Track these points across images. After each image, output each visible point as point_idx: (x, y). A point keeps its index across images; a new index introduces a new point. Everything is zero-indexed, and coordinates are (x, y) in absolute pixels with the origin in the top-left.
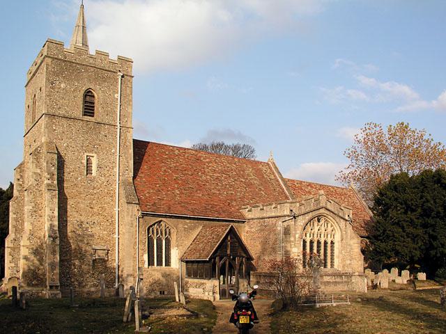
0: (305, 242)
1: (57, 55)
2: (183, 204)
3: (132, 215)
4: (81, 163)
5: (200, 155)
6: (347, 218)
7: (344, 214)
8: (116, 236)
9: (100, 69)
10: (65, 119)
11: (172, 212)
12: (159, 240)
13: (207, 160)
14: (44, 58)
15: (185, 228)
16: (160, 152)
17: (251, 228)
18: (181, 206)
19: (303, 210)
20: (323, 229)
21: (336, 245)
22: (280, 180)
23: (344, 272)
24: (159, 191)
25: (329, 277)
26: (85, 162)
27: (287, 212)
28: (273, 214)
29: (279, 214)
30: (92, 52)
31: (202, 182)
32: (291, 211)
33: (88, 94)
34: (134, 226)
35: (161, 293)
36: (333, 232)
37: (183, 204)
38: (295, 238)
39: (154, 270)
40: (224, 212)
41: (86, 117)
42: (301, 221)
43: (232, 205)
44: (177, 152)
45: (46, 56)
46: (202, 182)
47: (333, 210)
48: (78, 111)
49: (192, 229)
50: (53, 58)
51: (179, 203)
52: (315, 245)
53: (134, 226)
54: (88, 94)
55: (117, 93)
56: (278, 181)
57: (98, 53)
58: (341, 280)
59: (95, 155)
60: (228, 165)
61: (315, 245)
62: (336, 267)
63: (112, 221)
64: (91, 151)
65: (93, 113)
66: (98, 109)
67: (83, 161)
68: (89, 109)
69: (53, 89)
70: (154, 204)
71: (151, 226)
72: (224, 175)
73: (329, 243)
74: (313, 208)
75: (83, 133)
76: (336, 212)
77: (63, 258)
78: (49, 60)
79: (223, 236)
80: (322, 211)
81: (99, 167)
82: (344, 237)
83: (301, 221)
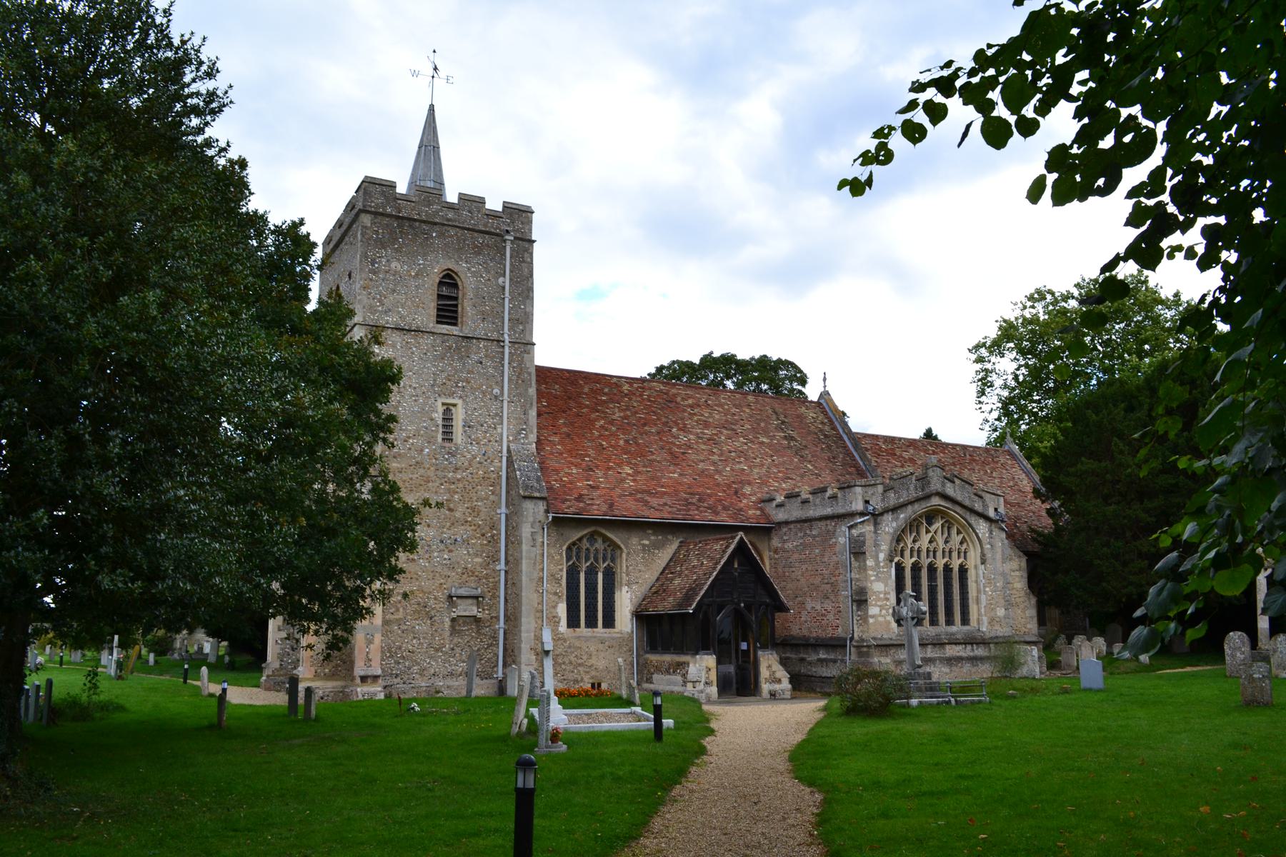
0: (900, 569)
1: (384, 207)
2: (639, 496)
3: (534, 522)
4: (432, 420)
5: (674, 391)
6: (991, 514)
7: (985, 506)
8: (502, 566)
9: (468, 229)
10: (398, 333)
11: (616, 512)
12: (591, 572)
13: (690, 401)
14: (357, 215)
15: (644, 545)
16: (592, 390)
17: (784, 541)
18: (636, 500)
19: (892, 499)
20: (940, 541)
21: (971, 575)
22: (845, 438)
23: (993, 634)
24: (591, 470)
25: (960, 647)
26: (438, 416)
27: (859, 506)
28: (828, 511)
29: (841, 510)
30: (452, 197)
31: (679, 447)
32: (867, 502)
33: (449, 281)
34: (538, 544)
35: (593, 685)
36: (965, 546)
37: (639, 496)
38: (877, 562)
39: (579, 637)
40: (725, 508)
41: (439, 326)
42: (890, 525)
43: (744, 495)
44: (626, 387)
45: (361, 211)
46: (679, 447)
47: (959, 498)
48: (426, 316)
49: (658, 546)
50: (376, 214)
51: (631, 494)
52: (924, 574)
53: (538, 544)
54: (449, 281)
55: (504, 275)
56: (841, 438)
57: (462, 197)
58: (986, 654)
59: (459, 402)
60: (734, 410)
61: (924, 574)
62: (973, 622)
63: (493, 536)
64: (451, 395)
65: (456, 318)
66: (467, 308)
67: (435, 415)
68: (448, 312)
69: (374, 273)
70: (580, 498)
71: (574, 544)
72: (725, 432)
73: (956, 569)
74: (913, 494)
75: (436, 358)
76: (967, 503)
77: (389, 617)
78: (366, 219)
79: (722, 562)
80: (936, 501)
81: (467, 425)
82: (989, 555)
83: (890, 525)
